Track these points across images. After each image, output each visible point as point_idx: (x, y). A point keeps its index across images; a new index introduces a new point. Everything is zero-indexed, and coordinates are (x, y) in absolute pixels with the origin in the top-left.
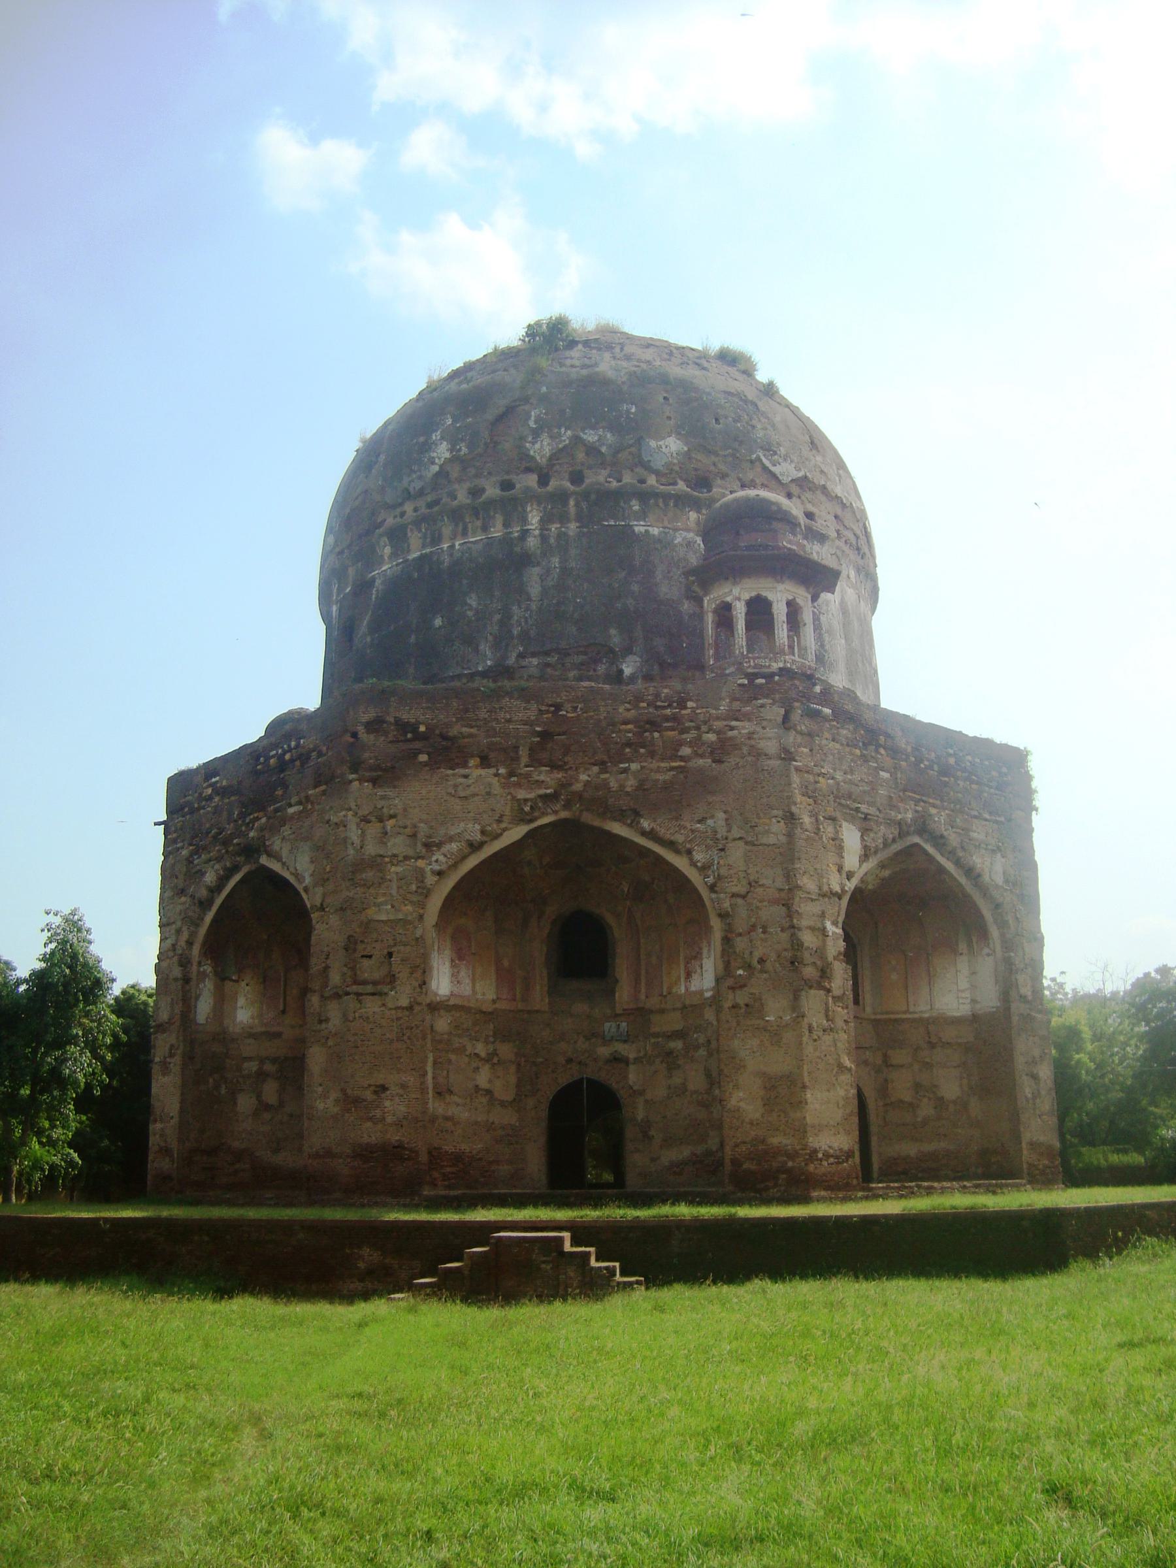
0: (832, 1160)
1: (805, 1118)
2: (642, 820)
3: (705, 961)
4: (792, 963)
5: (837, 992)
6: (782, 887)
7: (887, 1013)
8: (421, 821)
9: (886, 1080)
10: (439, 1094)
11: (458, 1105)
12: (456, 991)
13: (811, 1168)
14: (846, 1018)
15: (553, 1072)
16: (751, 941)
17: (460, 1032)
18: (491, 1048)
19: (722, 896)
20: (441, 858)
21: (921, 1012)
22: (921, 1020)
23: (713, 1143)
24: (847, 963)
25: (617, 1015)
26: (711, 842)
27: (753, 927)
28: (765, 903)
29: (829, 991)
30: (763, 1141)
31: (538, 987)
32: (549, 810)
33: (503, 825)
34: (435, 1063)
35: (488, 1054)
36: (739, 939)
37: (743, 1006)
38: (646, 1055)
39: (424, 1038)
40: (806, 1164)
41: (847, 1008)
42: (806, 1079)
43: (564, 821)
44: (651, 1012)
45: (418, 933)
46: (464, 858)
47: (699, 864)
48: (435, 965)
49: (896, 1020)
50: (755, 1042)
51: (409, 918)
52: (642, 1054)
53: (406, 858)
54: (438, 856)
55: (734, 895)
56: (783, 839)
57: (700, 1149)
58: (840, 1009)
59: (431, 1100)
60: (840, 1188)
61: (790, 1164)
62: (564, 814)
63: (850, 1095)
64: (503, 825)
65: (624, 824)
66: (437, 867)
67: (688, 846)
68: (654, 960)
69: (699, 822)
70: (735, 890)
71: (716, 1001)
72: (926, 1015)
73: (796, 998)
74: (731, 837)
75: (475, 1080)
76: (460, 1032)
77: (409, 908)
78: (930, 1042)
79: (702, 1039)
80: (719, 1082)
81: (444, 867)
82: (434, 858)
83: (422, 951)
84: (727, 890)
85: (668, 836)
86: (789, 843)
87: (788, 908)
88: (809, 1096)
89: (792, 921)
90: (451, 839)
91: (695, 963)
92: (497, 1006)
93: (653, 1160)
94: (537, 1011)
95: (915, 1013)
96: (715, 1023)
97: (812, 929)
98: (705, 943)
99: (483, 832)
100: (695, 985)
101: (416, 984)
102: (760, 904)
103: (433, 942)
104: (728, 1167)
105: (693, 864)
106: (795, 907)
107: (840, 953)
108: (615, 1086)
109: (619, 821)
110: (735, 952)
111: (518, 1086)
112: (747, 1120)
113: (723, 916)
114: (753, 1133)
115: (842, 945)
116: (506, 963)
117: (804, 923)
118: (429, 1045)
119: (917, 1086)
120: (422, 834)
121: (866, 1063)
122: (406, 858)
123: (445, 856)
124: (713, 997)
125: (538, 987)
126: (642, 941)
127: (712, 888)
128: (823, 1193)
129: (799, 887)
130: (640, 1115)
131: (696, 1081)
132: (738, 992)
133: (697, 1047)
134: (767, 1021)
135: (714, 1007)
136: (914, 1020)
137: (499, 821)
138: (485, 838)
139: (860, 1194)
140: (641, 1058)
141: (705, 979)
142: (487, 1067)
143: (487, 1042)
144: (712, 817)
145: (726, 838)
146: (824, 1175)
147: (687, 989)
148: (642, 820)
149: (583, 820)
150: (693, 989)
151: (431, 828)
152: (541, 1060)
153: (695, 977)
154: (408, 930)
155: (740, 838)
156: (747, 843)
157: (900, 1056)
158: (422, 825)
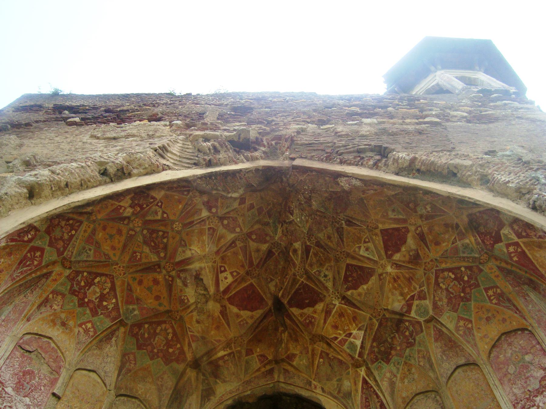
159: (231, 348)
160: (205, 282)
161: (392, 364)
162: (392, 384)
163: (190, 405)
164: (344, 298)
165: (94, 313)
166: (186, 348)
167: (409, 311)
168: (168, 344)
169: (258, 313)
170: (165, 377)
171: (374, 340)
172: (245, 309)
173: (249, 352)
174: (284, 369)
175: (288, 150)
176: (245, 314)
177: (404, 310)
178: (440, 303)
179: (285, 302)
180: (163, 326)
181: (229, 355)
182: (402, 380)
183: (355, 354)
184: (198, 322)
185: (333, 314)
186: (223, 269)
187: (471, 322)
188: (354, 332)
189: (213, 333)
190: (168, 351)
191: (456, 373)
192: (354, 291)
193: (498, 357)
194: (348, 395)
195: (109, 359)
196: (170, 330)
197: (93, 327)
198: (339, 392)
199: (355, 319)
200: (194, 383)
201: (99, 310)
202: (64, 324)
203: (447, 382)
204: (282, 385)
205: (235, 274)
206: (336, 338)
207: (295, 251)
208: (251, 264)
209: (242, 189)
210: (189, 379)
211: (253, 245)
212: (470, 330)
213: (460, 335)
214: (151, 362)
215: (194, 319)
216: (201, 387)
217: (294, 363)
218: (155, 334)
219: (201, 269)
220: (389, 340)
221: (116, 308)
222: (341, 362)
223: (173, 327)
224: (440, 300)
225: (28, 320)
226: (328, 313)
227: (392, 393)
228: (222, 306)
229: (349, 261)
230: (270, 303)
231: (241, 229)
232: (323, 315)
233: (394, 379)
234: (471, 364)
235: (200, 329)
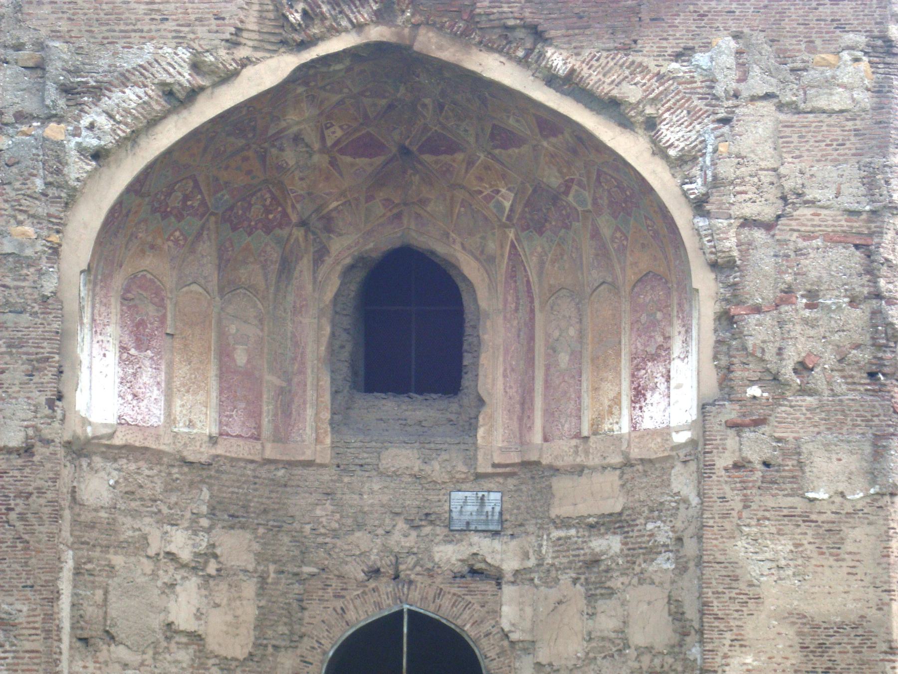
2: (550, 51)
3: (677, 367)
6: (855, 207)
8: (56, 35)
10: (85, 640)
11: (126, 666)
12: (130, 414)
15: (337, 596)
16: (781, 323)
17: (134, 505)
18: (203, 542)
19: (722, 223)
20: (102, 121)
25: (479, 476)
26: (701, 104)
27: (789, 291)
28: (818, 242)
31: (310, 412)
32: (344, 23)
33: (242, 53)
34: (78, 572)
35: (197, 555)
36: (753, 319)
37: (760, 467)
39: (56, 517)
43: (379, 48)
44: (555, 470)
45: (49, 286)
46: (153, 122)
47: (672, 152)
48: (84, 357)
50: (784, 546)
51: (29, 252)
52: (532, 562)
53: (21, 117)
54: (94, 116)
55: (747, 223)
56: (865, 99)
59: (65, 657)
62: (377, 33)
64: (242, 53)
65: (510, 57)
66: (92, 142)
67: (649, 110)
68: (564, 359)
69: (678, 57)
70: (749, 210)
74: (745, 94)
75: (166, 610)
76: (134, 505)
77: (29, 229)
80: (701, 632)
81: (108, 141)
82: (85, 121)
83: (55, 326)
84: (735, 211)
85: (607, 88)
86: (879, 108)
89: (874, 281)
90: (124, 80)
91: (656, 369)
92: (219, 450)
94: (309, 464)
96: (694, 500)
98: (677, 327)
99: (196, 67)
101: (42, 399)
102: (801, 244)
103: (81, 309)
105: (660, 151)
106: (885, 253)
108: (470, 631)
109: (500, 51)
110: (745, 348)
111: (260, 625)
116: (241, 358)
118: (66, 534)
120: (59, 64)
122: (21, 117)
123: (111, 117)
124: (693, 443)
125: (310, 412)
126: (539, 317)
127: (699, 206)
132: (748, 434)
133: (652, 552)
134: (812, 500)
135: (693, 466)
137: (233, 43)
138: (200, 81)
140: (529, 570)
142: (194, 581)
143: (194, 529)
144: (707, 46)
145: (736, 96)
147: (634, 427)
148: (550, 51)
149: (417, 47)
150: (647, 424)
151: (79, 51)
152: (307, 569)
153: (653, 398)
154: (25, 278)
155: (768, 96)
156: (780, 107)
158: (57, 44)
159: (345, 196)
160: (307, 140)
161: (545, 239)
162: (542, 263)
163: (301, 271)
164: (490, 153)
165: (180, 217)
166: (289, 210)
167: (566, 193)
168: (267, 211)
169: (379, 160)
170: (268, 249)
171: (526, 205)
172: (362, 156)
173: (370, 198)
174: (416, 213)
175: (410, 6)
176: (362, 161)
177: (562, 189)
178: (599, 201)
179: (414, 149)
180: (259, 194)
181: (344, 204)
182: (553, 262)
183: (503, 216)
184: (302, 179)
185: (477, 164)
186: (329, 125)
187: (627, 239)
188: (504, 190)
189: (321, 185)
190: (267, 218)
191: (602, 287)
192: (503, 151)
193: (638, 297)
194: (491, 259)
195: (205, 260)
196: (268, 195)
197: (182, 234)
198: (482, 252)
199: (504, 176)
200: (303, 245)
201: (185, 213)
202: (152, 247)
203: (591, 295)
204: (414, 234)
205: (345, 127)
206: (481, 192)
207: (424, 106)
208: (366, 117)
209: (348, 60)
210: (297, 240)
211: (367, 101)
212: (625, 247)
213: (614, 248)
214: (250, 239)
215: (297, 178)
216: (312, 250)
217: (429, 209)
218: (250, 205)
219: (301, 130)
220: (545, 211)
221: (203, 203)
222: (486, 218)
223: (270, 191)
224: (601, 198)
225: (121, 266)
226: (470, 163)
227: (540, 273)
228: (331, 157)
229: (496, 122)
230: (394, 150)
231: (350, 90)
232: (464, 165)
233: (545, 258)
234: (614, 287)
235: (304, 185)
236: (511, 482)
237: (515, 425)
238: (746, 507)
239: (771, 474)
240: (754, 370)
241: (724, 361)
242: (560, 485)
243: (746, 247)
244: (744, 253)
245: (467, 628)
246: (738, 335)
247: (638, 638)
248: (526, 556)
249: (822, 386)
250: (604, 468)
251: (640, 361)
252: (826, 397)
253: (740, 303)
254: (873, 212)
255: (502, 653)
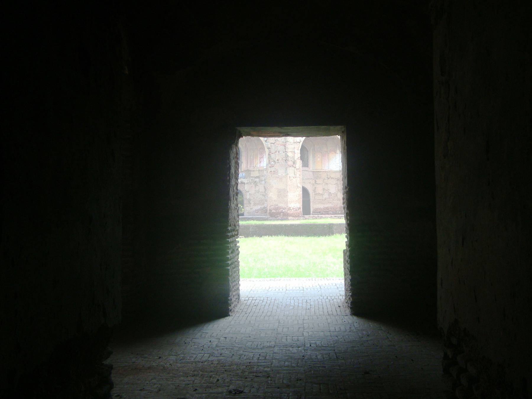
0: (294, 210)
1: (287, 199)
3: (264, 159)
4: (286, 161)
5: (297, 168)
6: (283, 141)
7: (316, 169)
9: (315, 188)
13: (289, 212)
14: (299, 174)
19: (268, 143)
21: (326, 169)
22: (325, 172)
23: (265, 205)
24: (301, 160)
25: (242, 171)
29: (295, 167)
30: (277, 205)
36: (272, 154)
37: (273, 172)
38: (249, 182)
40: (288, 211)
41: (300, 171)
42: (288, 190)
44: (251, 171)
49: (319, 171)
55: (271, 143)
57: (262, 207)
58: (298, 172)
60: (296, 216)
61: (284, 211)
63: (300, 194)
68: (252, 157)
71: (266, 169)
72: (327, 170)
73: (286, 170)
78: (327, 178)
79: (263, 179)
84: (270, 142)
87: (285, 147)
88: (289, 193)
89: (286, 150)
93: (251, 209)
95: (323, 170)
97: (291, 152)
98: (264, 155)
100: (262, 165)
102: (278, 146)
104: (268, 212)
106: (286, 147)
107: (299, 158)
110: (271, 158)
112: (273, 200)
113: (269, 148)
114: (275, 203)
115: (299, 155)
117: (289, 150)
119: (324, 189)
121: (310, 183)
128: (292, 218)
129: (288, 141)
130: (248, 197)
131: (262, 190)
132: (272, 168)
133: (262, 181)
136: (324, 171)
139: (302, 218)
141: (264, 163)
146: (292, 213)
147: (260, 166)
150: (261, 166)
153: (262, 163)
157: (318, 181)
236: (246, 172)
237: (246, 165)
238: (271, 176)
239: (274, 172)
240: (272, 161)
241: (269, 159)
242: (252, 173)
243: (271, 146)
244: (271, 147)
245: (241, 189)
246: (270, 156)
247: (261, 191)
248: (248, 181)
249: (280, 162)
250: (257, 171)
251: (260, 158)
252: (281, 164)
253: (271, 153)
254: (285, 142)
255: (245, 192)
